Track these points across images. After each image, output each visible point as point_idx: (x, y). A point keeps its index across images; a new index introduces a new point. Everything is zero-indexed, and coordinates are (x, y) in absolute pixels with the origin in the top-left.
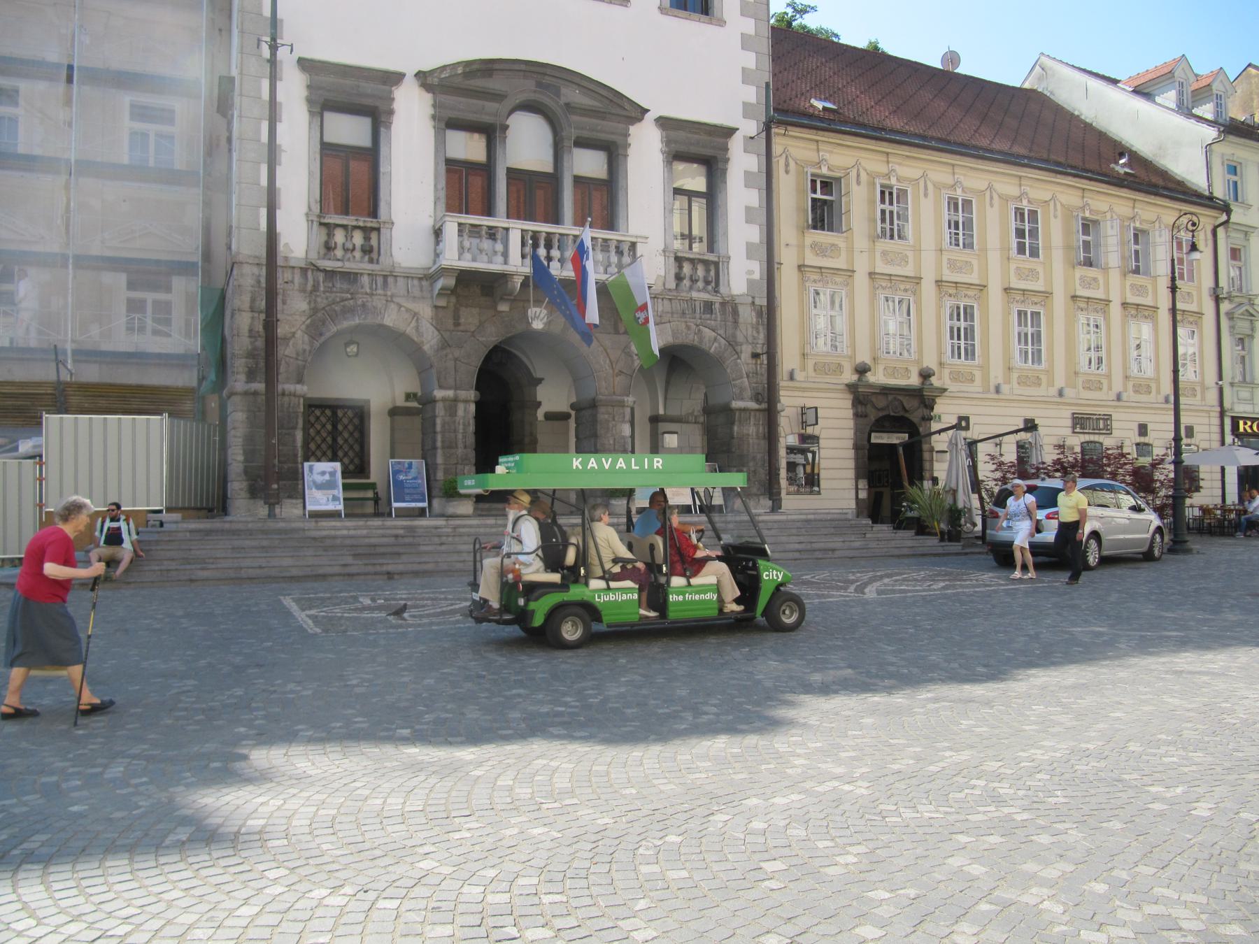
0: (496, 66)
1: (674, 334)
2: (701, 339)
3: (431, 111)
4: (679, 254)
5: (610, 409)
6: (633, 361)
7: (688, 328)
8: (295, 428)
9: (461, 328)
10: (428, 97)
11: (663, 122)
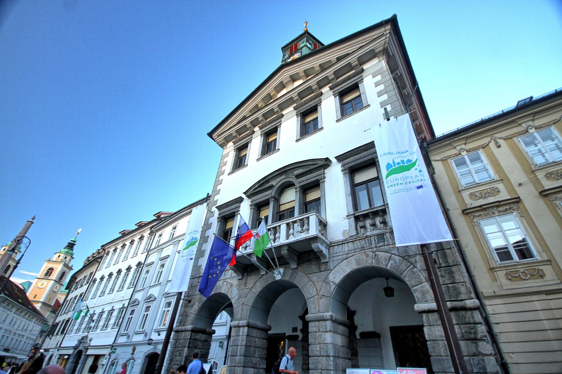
0: (268, 178)
1: (358, 263)
2: (378, 261)
3: (250, 203)
4: (357, 215)
5: (317, 323)
6: (330, 287)
7: (367, 256)
8: (185, 347)
9: (247, 287)
10: (250, 200)
11: (340, 158)
